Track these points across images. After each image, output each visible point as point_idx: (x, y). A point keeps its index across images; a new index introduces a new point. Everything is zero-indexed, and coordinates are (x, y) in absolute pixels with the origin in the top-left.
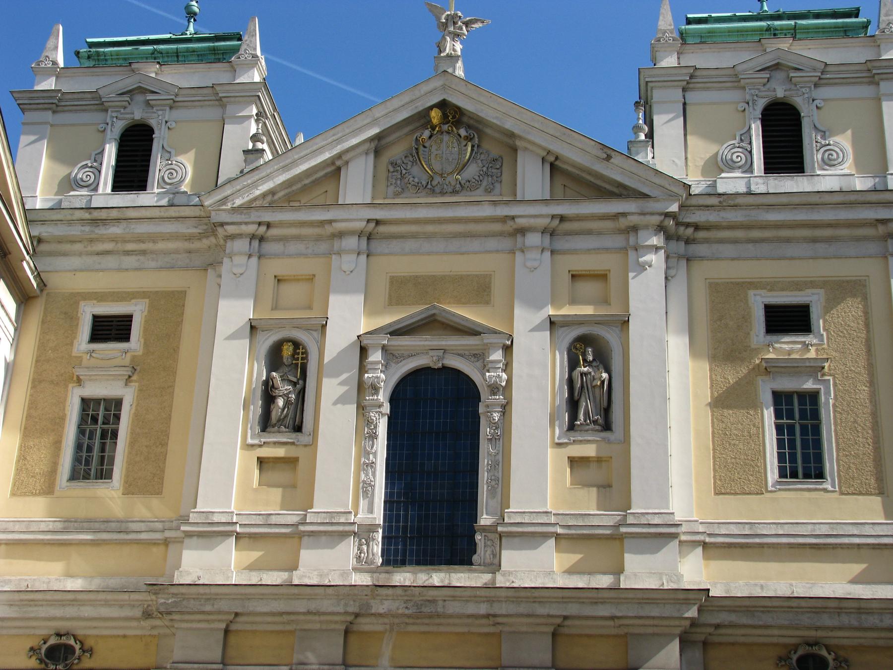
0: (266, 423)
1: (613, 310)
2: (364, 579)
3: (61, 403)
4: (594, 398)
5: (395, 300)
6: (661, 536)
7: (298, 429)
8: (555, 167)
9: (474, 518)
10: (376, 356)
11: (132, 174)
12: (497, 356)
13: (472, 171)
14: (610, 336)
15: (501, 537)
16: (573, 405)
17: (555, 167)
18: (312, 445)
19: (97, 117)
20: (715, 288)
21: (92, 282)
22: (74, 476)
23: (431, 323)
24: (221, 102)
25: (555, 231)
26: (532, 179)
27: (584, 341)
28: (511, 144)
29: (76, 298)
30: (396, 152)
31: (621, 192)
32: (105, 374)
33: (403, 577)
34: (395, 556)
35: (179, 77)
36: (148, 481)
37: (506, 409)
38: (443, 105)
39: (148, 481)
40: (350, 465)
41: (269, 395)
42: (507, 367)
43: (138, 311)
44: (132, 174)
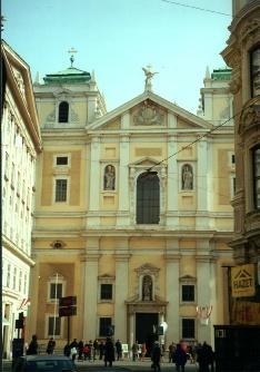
0: (105, 188)
1: (193, 158)
2: (133, 228)
3: (51, 181)
4: (188, 179)
5: (137, 155)
6: (206, 216)
7: (113, 189)
8: (178, 118)
9: (158, 210)
10: (132, 170)
11: (63, 117)
12: (164, 170)
13: (156, 118)
14: (192, 164)
15: (165, 217)
16: (183, 182)
17: (178, 118)
18: (117, 193)
19: (52, 100)
20: (220, 151)
21: (56, 148)
22: (57, 200)
23: (147, 161)
24: (87, 96)
25: (179, 135)
26: (172, 122)
27: (186, 165)
28: (166, 111)
29: (51, 153)
30: (135, 113)
31: (193, 125)
32: (62, 172)
33: (142, 227)
34: (140, 221)
35: (72, 88)
36: (75, 202)
37: (166, 183)
38: (148, 100)
39: (75, 202)
40: (126, 198)
41: (106, 181)
42: (166, 173)
43: (69, 156)
44: (63, 117)
